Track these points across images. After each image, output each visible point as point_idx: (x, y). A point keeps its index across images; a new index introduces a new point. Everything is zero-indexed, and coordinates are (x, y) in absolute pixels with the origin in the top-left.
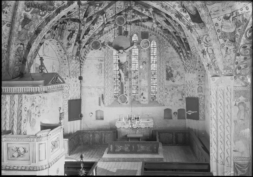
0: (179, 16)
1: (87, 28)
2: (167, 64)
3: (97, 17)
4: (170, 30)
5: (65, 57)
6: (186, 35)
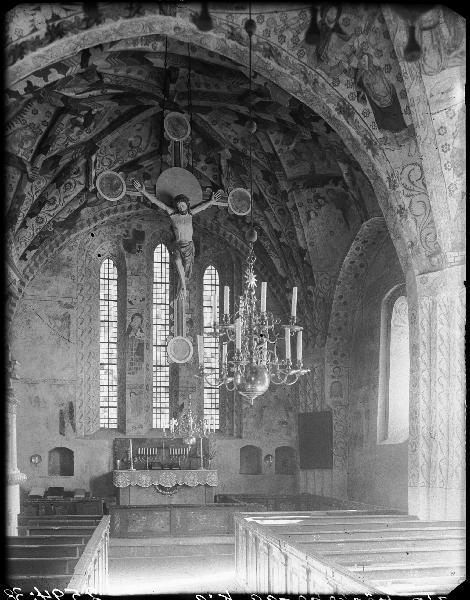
0: (346, 111)
1: (38, 194)
3: (74, 162)
4: (265, 228)
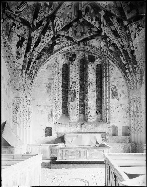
1: (37, 38)
2: (113, 84)
4: (118, 45)
5: (14, 67)
6: (134, 47)
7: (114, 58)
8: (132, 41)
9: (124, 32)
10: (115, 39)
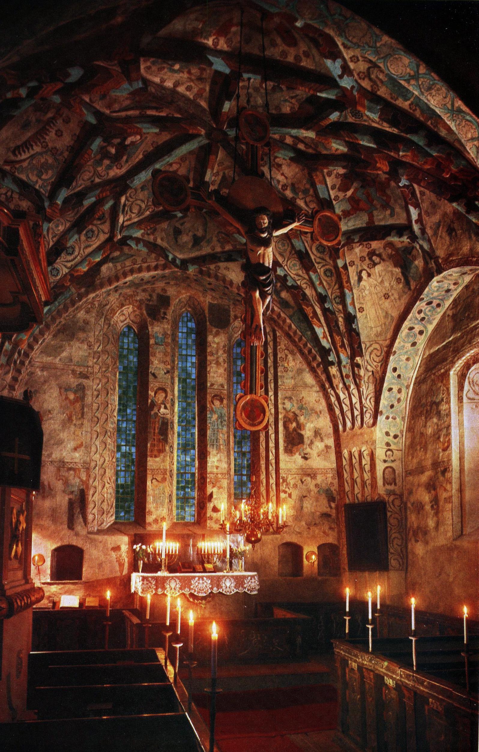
1: (55, 239)
2: (288, 405)
3: (100, 202)
4: (309, 292)
6: (357, 306)
7: (293, 326)
8: (351, 290)
9: (328, 260)
10: (300, 273)
